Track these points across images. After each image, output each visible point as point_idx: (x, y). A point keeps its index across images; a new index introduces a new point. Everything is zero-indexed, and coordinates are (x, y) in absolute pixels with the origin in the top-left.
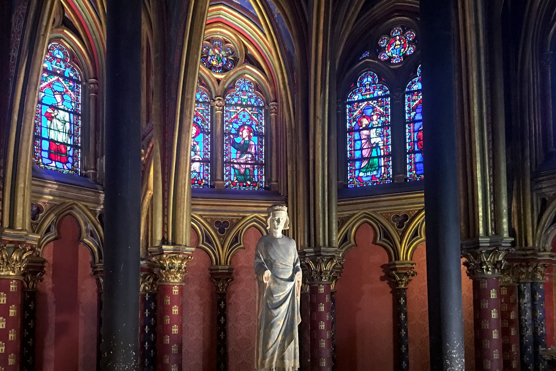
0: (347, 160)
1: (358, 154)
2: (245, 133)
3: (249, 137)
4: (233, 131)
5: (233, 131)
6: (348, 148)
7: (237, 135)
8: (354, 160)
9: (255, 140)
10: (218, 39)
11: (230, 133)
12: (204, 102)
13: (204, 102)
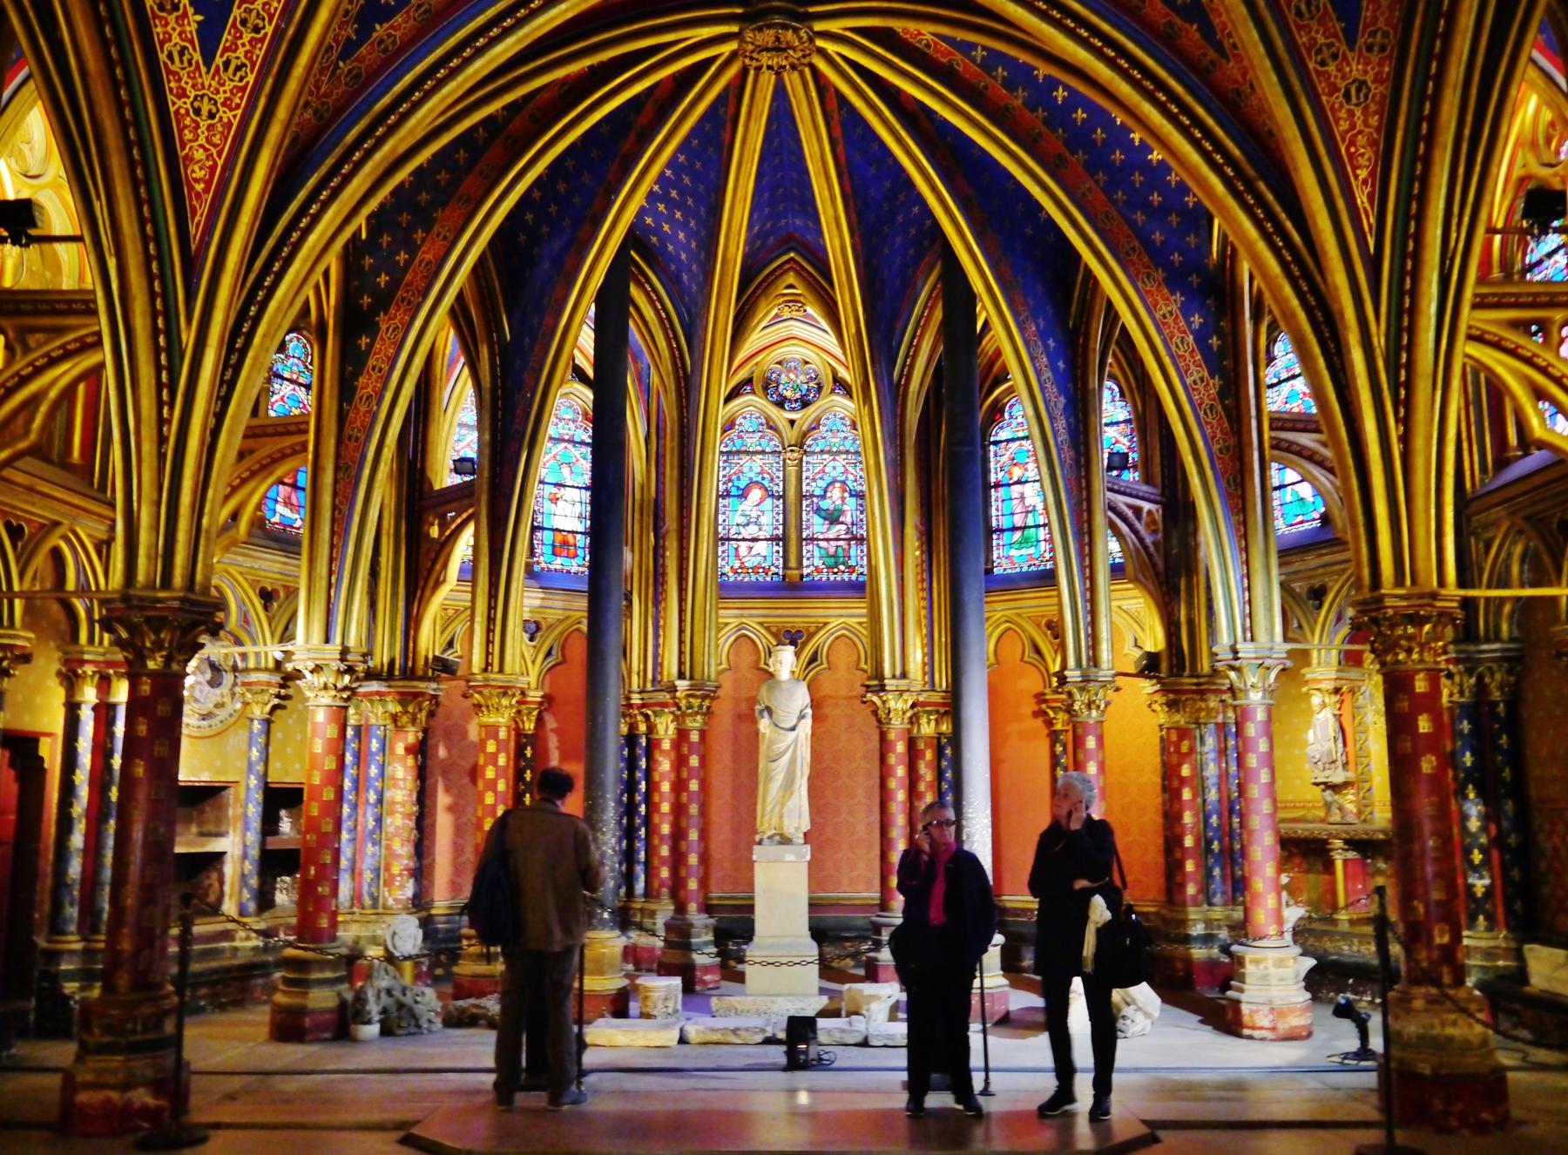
0: (990, 531)
1: (1006, 523)
2: (836, 493)
3: (843, 499)
4: (818, 492)
5: (818, 492)
6: (994, 512)
7: (823, 497)
9: (851, 503)
10: (793, 360)
11: (812, 496)
12: (773, 452)
13: (773, 452)
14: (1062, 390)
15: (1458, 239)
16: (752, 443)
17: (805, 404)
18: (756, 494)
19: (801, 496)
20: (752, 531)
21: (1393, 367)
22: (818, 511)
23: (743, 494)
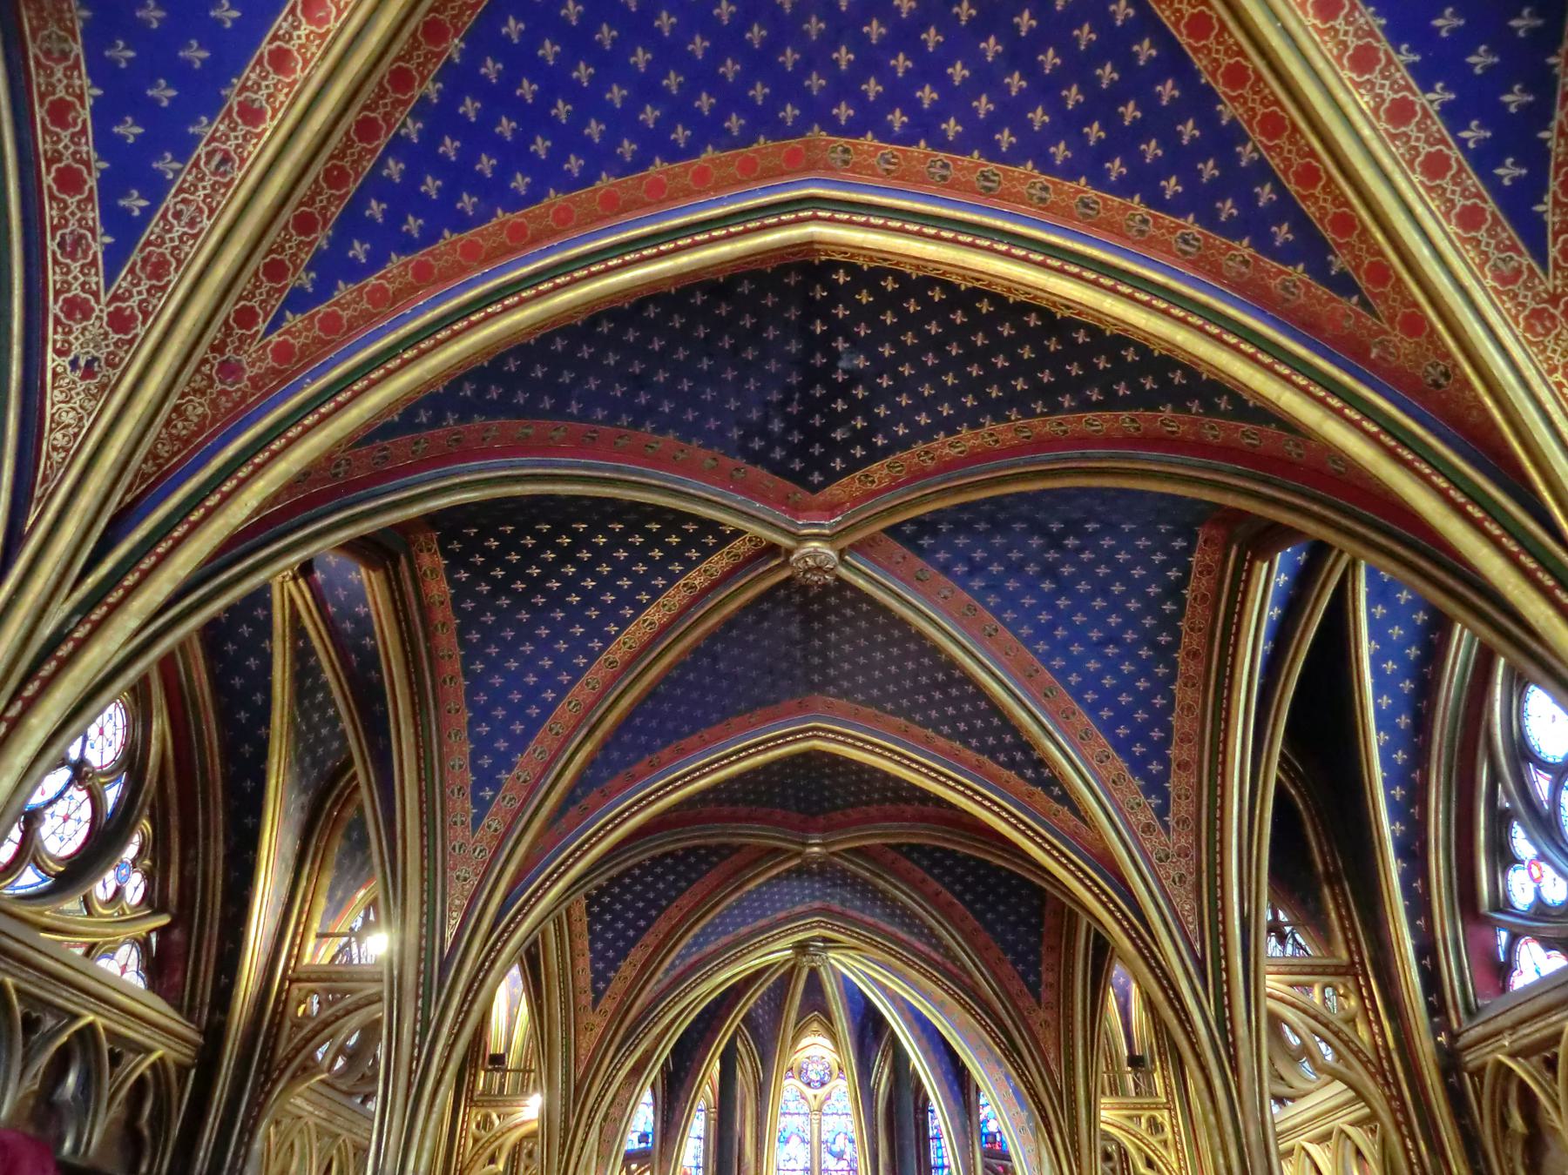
1: (940, 1162)
8: (937, 1168)
9: (850, 1146)
14: (956, 1100)
15: (1092, 1084)
16: (792, 1107)
17: (823, 1084)
18: (795, 1140)
19: (821, 1142)
20: (791, 1165)
21: (1073, 1146)
22: (831, 1152)
23: (787, 1141)
